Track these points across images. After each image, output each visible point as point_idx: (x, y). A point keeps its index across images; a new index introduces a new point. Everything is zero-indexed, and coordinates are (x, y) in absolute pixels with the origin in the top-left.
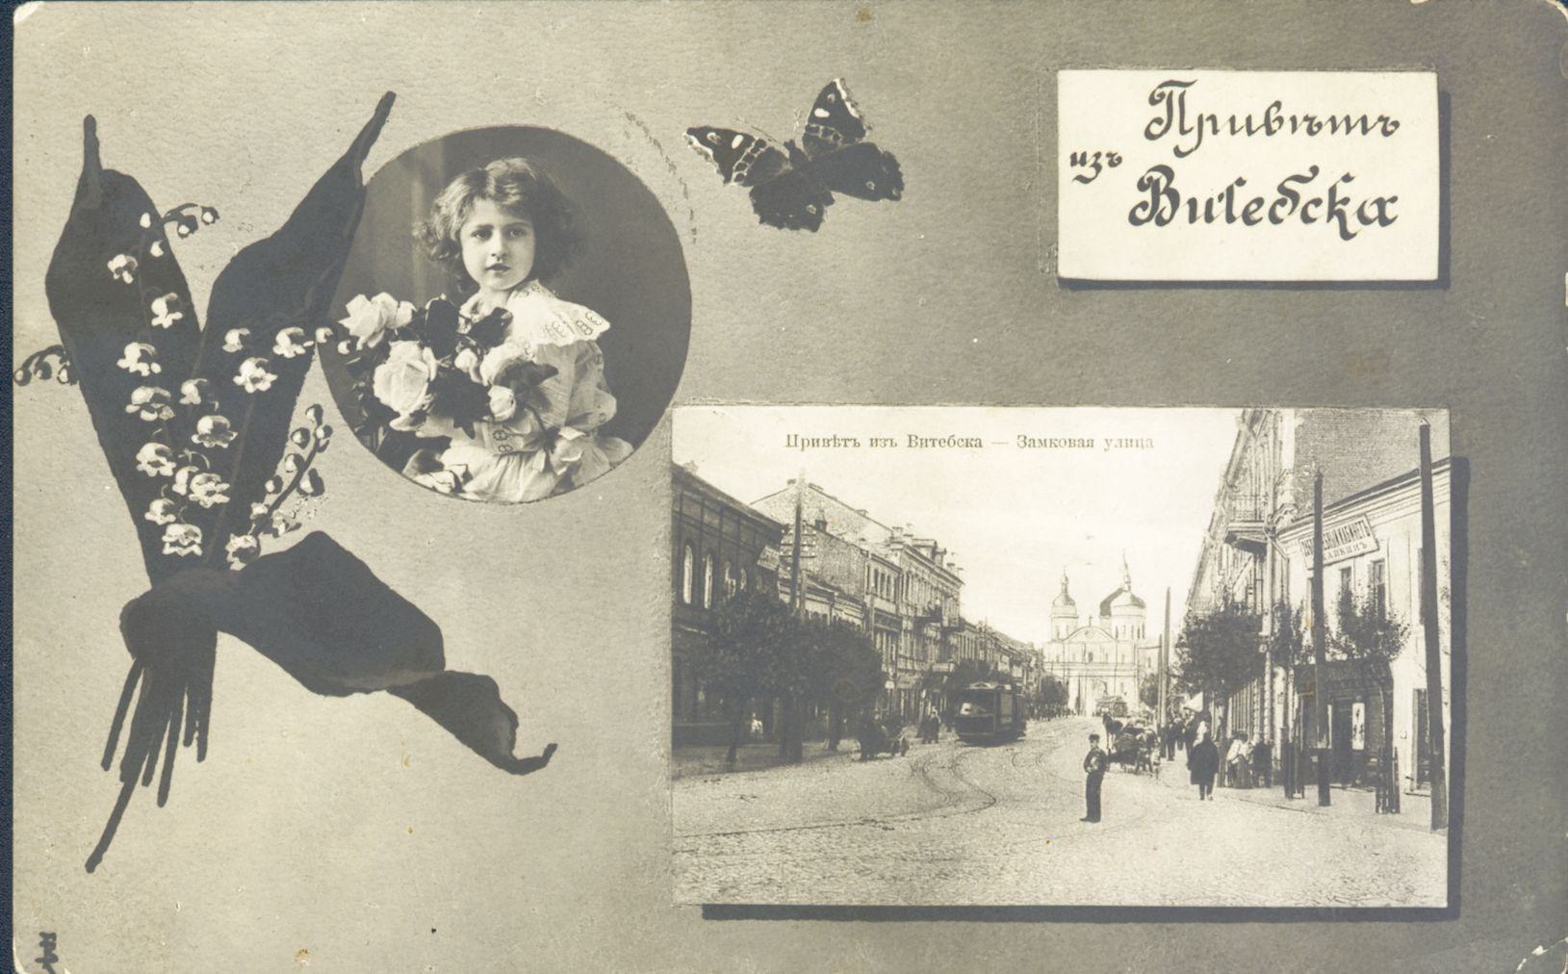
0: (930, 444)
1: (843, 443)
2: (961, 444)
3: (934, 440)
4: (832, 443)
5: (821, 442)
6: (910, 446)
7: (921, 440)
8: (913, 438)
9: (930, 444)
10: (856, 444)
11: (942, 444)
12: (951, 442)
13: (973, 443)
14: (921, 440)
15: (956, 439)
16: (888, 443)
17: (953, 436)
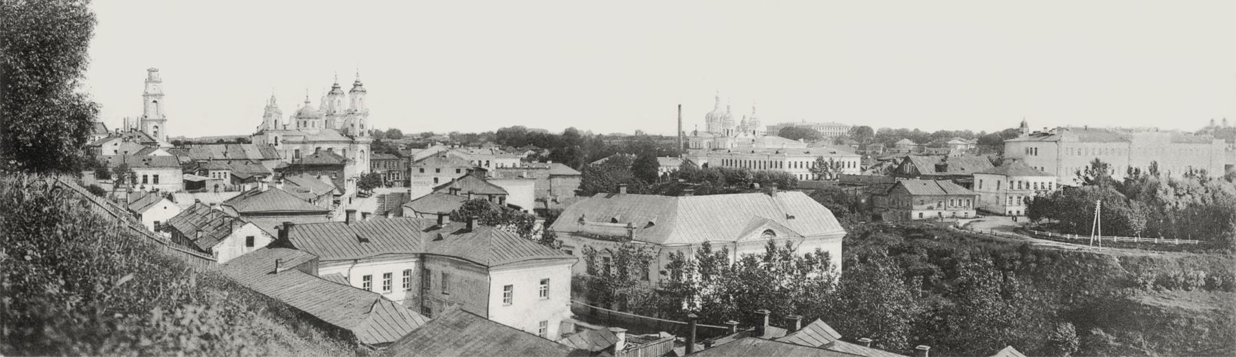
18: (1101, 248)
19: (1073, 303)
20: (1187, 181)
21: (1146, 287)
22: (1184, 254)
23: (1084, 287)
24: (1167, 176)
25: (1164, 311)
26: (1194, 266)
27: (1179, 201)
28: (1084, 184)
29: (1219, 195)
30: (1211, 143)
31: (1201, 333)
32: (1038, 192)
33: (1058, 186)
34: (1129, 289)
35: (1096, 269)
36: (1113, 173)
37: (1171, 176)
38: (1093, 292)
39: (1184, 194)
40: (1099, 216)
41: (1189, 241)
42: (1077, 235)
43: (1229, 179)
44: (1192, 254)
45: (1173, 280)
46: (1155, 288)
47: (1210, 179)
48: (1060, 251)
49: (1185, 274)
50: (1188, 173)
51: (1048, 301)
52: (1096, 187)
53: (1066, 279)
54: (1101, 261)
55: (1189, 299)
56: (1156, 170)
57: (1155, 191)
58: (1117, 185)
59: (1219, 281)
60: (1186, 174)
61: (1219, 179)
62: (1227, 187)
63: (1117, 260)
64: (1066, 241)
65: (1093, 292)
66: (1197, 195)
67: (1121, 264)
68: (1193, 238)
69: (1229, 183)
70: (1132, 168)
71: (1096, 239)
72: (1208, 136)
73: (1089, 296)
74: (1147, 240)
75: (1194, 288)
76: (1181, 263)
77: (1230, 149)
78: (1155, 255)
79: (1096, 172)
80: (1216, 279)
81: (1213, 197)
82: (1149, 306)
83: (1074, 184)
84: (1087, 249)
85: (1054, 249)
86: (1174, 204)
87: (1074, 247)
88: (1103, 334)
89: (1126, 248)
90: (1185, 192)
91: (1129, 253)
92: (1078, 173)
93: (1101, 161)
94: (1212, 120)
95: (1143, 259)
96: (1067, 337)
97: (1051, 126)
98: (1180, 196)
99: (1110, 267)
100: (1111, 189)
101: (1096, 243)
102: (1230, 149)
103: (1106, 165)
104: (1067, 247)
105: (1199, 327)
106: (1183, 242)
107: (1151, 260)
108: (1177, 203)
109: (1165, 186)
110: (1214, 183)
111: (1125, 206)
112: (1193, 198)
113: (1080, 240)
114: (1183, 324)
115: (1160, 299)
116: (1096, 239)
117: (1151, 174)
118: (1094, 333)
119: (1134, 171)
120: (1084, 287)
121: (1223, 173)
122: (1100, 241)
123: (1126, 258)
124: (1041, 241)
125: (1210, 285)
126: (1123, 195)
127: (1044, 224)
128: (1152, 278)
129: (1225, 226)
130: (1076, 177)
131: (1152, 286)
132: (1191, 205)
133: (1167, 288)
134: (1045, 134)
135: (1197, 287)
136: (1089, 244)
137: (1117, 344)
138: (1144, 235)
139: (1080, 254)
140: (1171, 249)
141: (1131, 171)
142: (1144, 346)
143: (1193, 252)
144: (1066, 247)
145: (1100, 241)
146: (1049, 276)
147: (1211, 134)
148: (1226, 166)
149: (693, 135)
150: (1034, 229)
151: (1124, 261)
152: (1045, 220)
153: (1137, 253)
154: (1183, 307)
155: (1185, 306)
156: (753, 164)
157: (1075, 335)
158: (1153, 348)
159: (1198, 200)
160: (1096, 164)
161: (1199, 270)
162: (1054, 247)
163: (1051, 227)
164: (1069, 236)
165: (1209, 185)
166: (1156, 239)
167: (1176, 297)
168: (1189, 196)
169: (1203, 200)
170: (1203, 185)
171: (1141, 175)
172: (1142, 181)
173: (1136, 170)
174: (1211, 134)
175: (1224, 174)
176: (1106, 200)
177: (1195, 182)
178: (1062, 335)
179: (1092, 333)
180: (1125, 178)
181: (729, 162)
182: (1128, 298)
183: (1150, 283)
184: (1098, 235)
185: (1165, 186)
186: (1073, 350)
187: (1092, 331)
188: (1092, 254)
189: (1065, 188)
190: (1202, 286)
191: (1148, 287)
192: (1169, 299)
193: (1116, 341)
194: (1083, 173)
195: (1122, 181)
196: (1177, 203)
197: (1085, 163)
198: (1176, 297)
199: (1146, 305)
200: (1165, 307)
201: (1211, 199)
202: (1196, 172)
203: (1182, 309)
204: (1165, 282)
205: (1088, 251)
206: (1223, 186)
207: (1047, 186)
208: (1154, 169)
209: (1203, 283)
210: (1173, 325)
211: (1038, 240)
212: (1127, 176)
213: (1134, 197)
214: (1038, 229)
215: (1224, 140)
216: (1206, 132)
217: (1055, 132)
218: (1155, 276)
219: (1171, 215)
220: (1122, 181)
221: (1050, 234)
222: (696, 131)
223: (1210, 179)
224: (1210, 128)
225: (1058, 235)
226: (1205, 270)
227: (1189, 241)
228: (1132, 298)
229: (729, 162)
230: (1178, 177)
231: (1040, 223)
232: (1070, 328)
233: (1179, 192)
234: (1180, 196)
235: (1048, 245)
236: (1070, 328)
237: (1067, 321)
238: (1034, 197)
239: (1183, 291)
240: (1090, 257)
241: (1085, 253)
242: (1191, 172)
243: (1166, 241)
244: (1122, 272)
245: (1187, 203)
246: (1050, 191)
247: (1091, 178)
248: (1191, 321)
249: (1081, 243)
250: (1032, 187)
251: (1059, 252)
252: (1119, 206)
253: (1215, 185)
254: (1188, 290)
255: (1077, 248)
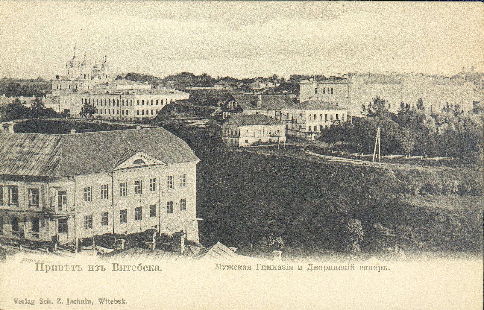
0: (126, 269)
1: (71, 269)
2: (146, 269)
3: (129, 266)
4: (65, 268)
5: (58, 268)
6: (114, 270)
7: (121, 266)
8: (116, 265)
9: (126, 269)
10: (80, 269)
11: (134, 269)
12: (140, 268)
13: (154, 268)
14: (121, 266)
15: (142, 265)
16: (100, 268)
17: (141, 264)
18: (380, 163)
19: (360, 204)
20: (445, 113)
21: (414, 192)
22: (443, 168)
23: (368, 193)
24: (430, 109)
25: (427, 211)
26: (450, 177)
27: (439, 128)
28: (368, 116)
29: (469, 123)
30: (462, 85)
31: (455, 227)
32: (334, 122)
33: (349, 117)
34: (401, 194)
35: (377, 179)
36: (389, 107)
37: (433, 110)
38: (375, 197)
39: (443, 123)
40: (379, 140)
41: (446, 158)
42: (362, 154)
43: (476, 111)
44: (448, 168)
45: (435, 187)
46: (421, 193)
47: (462, 112)
48: (350, 165)
49: (443, 182)
50: (446, 107)
51: (341, 203)
52: (376, 118)
53: (355, 186)
54: (381, 173)
55: (446, 201)
56: (421, 105)
57: (421, 121)
58: (392, 116)
59: (468, 188)
60: (444, 108)
61: (468, 111)
62: (476, 118)
63: (393, 172)
64: (355, 158)
65: (375, 197)
66: (452, 124)
67: (396, 175)
68: (450, 156)
69: (476, 115)
70: (404, 104)
71: (377, 157)
72: (461, 80)
73: (371, 199)
74: (415, 157)
75: (450, 193)
76: (440, 174)
77: (477, 89)
78: (421, 168)
79: (377, 107)
80: (466, 186)
81: (464, 125)
82: (417, 207)
83: (360, 116)
84: (370, 164)
85: (345, 164)
86: (435, 130)
87: (360, 163)
88: (382, 227)
89: (399, 163)
90: (443, 121)
91: (401, 167)
92: (364, 108)
93: (380, 99)
94: (464, 68)
95: (412, 172)
96: (355, 230)
97: (343, 71)
98: (439, 124)
99: (387, 178)
100: (388, 119)
101: (377, 160)
102: (477, 89)
103: (385, 101)
104: (355, 162)
105: (454, 222)
106: (442, 159)
107: (418, 172)
108: (437, 130)
109: (428, 117)
110: (465, 115)
111: (399, 132)
112: (449, 126)
113: (365, 157)
114: (442, 220)
115: (425, 201)
116: (377, 157)
117: (418, 108)
118: (376, 226)
119: (405, 106)
120: (368, 193)
121: (471, 107)
122: (380, 158)
123: (399, 171)
124: (336, 158)
125: (462, 191)
126: (396, 124)
127: (338, 146)
128: (418, 186)
129: (473, 147)
130: (362, 110)
131: (419, 192)
132: (448, 131)
133: (430, 193)
134: (339, 78)
135: (452, 192)
136: (371, 160)
137: (393, 235)
138: (412, 153)
139: (365, 168)
140: (432, 164)
141: (403, 106)
142: (413, 237)
143: (449, 167)
144: (354, 163)
145: (380, 158)
146: (342, 184)
147: (463, 78)
148: (474, 102)
149: (56, 79)
150: (330, 149)
151: (398, 173)
152: (339, 143)
153: (408, 167)
154: (441, 207)
155: (443, 206)
156: (95, 102)
157: (361, 229)
158: (419, 238)
159: (453, 127)
160: (377, 101)
161: (454, 180)
162: (346, 162)
163: (343, 148)
164: (356, 155)
165: (461, 116)
166: (422, 157)
167: (436, 200)
168: (447, 125)
169: (457, 128)
170: (457, 116)
171: (410, 109)
172: (412, 113)
173: (407, 105)
174: (463, 78)
175: (473, 108)
176: (385, 127)
177: (451, 114)
178: (351, 228)
179: (374, 227)
180: (398, 111)
181: (104, 102)
182: (401, 201)
183: (417, 189)
184: (378, 154)
185: (428, 117)
186: (359, 239)
187: (374, 226)
188: (374, 168)
189: (354, 118)
190: (456, 192)
191: (416, 193)
192: (431, 201)
193: (392, 233)
194: (367, 107)
195: (397, 113)
196: (437, 130)
197: (368, 100)
198: (436, 200)
199: (414, 206)
200: (428, 207)
201: (463, 127)
202: (452, 106)
203: (442, 209)
204: (428, 189)
205: (371, 166)
206: (471, 117)
207: (340, 117)
208: (420, 104)
209: (457, 189)
210: (434, 221)
211: (334, 158)
212: (400, 109)
213: (405, 125)
214: (334, 149)
215: (472, 83)
216: (459, 77)
217: (346, 77)
218: (421, 184)
219: (433, 139)
220: (397, 113)
221: (343, 153)
222: (58, 75)
223: (462, 112)
224: (462, 74)
225: (349, 154)
226: (458, 180)
227: (446, 158)
228: (404, 201)
229: (104, 102)
230: (438, 110)
231: (335, 144)
232: (358, 223)
233: (439, 121)
234: (439, 124)
235: (341, 161)
236: (358, 223)
237: (355, 218)
238: (331, 125)
239: (442, 195)
240: (372, 169)
241: (369, 167)
242: (448, 106)
243: (429, 158)
244: (396, 182)
245: (445, 129)
246: (343, 121)
247: (373, 111)
248: (448, 218)
249: (366, 160)
250: (329, 118)
251: (349, 166)
252: (394, 132)
253: (466, 116)
254: (445, 195)
255: (363, 163)
